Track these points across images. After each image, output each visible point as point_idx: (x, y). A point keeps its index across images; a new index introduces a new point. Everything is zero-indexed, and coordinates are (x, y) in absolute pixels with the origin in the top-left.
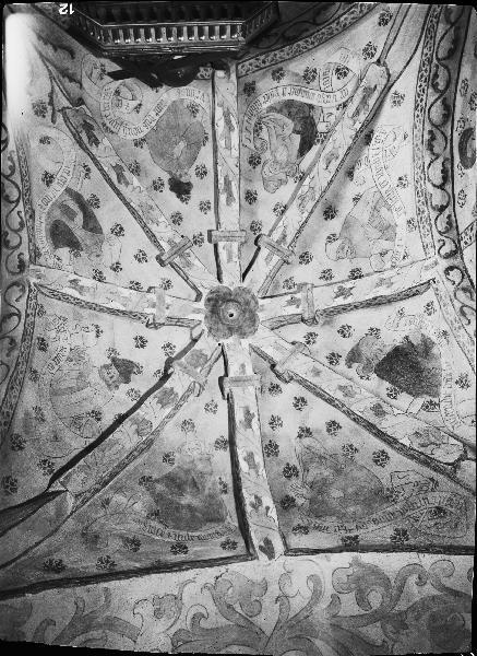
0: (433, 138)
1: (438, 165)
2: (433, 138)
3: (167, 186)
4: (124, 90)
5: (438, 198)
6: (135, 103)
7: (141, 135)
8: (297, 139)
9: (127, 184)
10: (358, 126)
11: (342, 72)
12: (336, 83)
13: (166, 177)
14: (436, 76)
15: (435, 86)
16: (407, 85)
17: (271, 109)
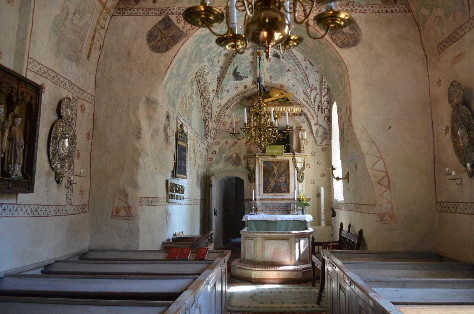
0: (205, 89)
1: (202, 84)
2: (205, 89)
3: (281, 57)
4: (292, 86)
5: (201, 78)
6: (289, 82)
7: (288, 73)
8: (238, 71)
9: (294, 66)
10: (223, 83)
11: (228, 91)
12: (229, 88)
13: (281, 59)
14: (207, 101)
15: (206, 99)
16: (212, 95)
17: (247, 77)
